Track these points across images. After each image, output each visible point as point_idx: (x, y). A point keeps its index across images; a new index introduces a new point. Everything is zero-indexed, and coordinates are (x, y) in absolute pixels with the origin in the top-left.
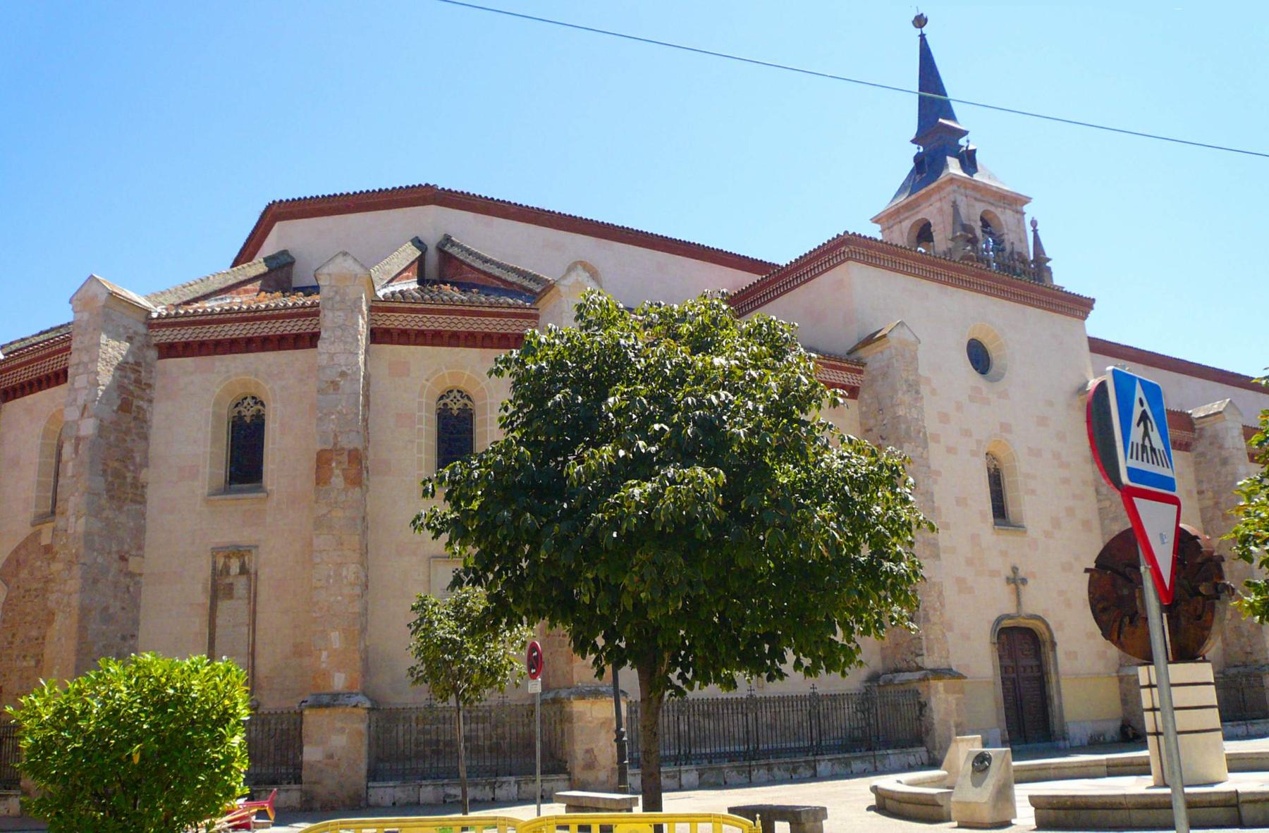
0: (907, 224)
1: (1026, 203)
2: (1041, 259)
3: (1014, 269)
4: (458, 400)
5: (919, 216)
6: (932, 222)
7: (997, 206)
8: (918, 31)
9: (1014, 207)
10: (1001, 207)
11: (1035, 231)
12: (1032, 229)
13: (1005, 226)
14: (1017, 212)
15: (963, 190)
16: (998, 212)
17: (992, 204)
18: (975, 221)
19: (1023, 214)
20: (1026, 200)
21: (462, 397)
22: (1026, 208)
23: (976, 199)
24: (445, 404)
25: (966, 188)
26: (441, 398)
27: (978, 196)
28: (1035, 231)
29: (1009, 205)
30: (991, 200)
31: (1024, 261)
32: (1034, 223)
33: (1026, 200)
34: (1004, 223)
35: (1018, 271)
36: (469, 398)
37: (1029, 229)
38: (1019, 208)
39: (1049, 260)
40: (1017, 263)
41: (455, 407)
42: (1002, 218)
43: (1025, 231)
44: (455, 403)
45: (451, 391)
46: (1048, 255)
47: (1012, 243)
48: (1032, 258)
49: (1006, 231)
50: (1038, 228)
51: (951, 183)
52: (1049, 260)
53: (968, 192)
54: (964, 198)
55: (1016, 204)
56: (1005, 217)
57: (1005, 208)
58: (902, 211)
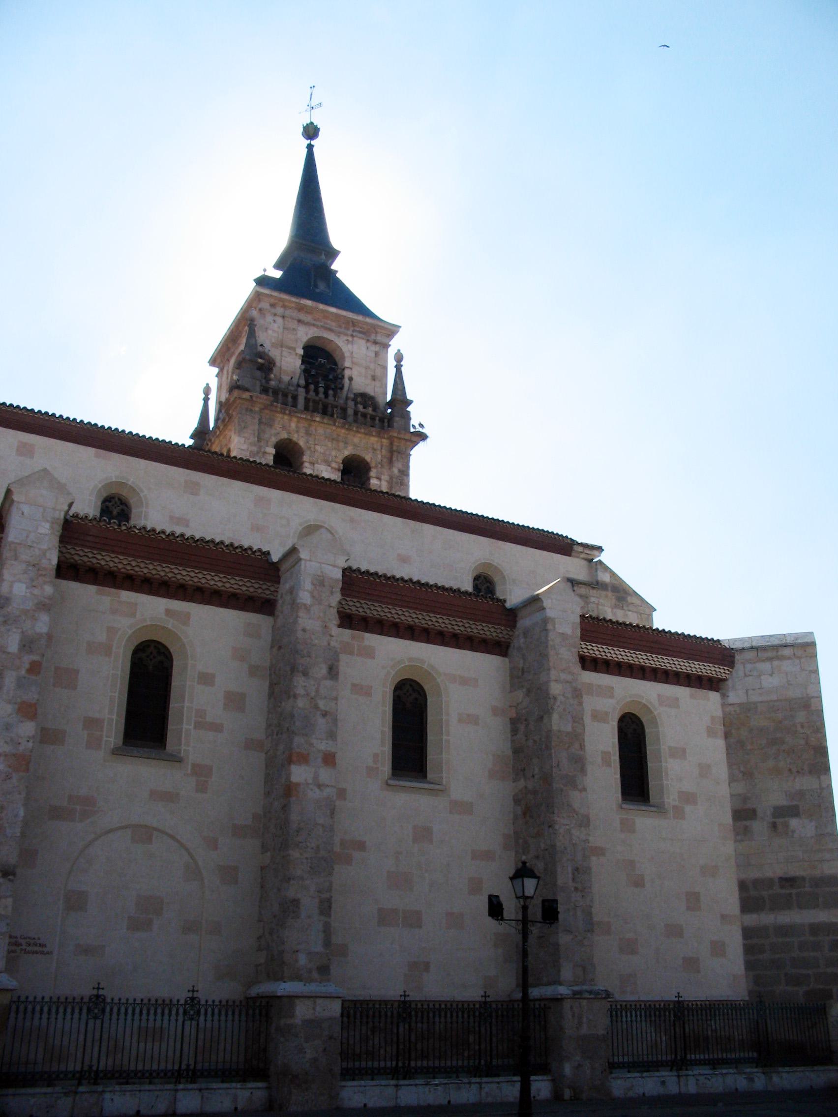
2: (400, 401)
7: (338, 334)
9: (373, 337)
10: (347, 335)
11: (398, 368)
12: (395, 363)
14: (375, 343)
18: (294, 349)
19: (386, 346)
23: (299, 321)
25: (284, 306)
28: (398, 368)
29: (360, 332)
30: (333, 325)
32: (399, 358)
33: (391, 331)
34: (347, 354)
38: (379, 338)
39: (409, 403)
42: (346, 348)
43: (385, 368)
46: (409, 396)
49: (347, 364)
53: (288, 312)
54: (280, 320)
55: (376, 333)
57: (352, 336)
58: (230, 345)
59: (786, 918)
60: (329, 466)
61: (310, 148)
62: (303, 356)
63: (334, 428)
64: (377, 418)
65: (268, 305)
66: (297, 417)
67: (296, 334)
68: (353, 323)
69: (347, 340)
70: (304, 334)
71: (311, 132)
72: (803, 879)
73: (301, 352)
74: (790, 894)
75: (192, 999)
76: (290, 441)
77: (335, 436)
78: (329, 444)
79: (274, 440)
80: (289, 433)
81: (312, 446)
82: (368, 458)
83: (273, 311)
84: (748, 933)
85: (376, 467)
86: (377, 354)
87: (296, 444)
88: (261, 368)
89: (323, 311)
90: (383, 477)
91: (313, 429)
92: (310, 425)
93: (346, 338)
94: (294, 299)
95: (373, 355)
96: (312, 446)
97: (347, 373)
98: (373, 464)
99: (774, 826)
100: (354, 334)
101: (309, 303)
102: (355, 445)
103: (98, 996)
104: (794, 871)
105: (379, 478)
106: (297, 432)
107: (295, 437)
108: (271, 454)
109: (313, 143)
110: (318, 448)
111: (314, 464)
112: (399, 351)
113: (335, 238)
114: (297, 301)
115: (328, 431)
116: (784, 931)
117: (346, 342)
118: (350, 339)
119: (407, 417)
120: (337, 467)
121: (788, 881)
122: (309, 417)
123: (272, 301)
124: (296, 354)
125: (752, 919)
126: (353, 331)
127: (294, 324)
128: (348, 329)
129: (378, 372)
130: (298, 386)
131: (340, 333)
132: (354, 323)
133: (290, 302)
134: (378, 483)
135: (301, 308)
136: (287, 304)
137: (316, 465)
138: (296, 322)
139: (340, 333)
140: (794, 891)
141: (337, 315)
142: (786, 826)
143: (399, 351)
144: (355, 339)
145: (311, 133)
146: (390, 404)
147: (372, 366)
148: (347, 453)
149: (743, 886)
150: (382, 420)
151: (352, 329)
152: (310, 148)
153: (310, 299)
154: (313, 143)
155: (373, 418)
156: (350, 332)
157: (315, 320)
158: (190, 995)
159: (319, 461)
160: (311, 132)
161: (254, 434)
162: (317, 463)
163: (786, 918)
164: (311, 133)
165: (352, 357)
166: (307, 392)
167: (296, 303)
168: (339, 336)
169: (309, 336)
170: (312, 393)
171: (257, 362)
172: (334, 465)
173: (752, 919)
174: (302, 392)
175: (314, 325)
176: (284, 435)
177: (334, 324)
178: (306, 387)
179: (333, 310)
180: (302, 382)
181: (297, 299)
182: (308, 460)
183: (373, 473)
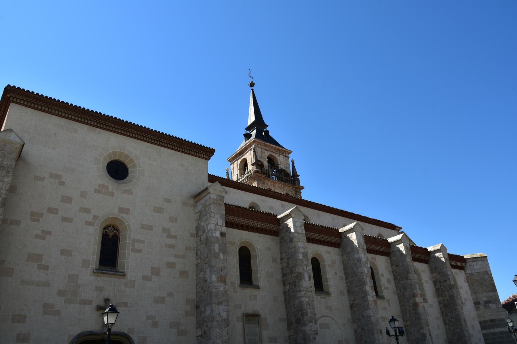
0: (239, 161)
1: (290, 153)
3: (282, 178)
4: (112, 231)
5: (243, 157)
6: (247, 159)
8: (251, 88)
10: (278, 154)
11: (293, 164)
13: (279, 162)
14: (285, 156)
15: (260, 146)
16: (276, 156)
18: (265, 159)
20: (290, 152)
21: (114, 230)
22: (289, 156)
23: (265, 150)
24: (106, 232)
25: (261, 145)
26: (105, 228)
27: (267, 149)
28: (293, 164)
29: (281, 153)
30: (274, 151)
31: (287, 174)
33: (290, 152)
34: (279, 160)
35: (284, 179)
36: (117, 231)
37: (291, 163)
38: (286, 155)
39: (299, 176)
40: (283, 176)
41: (111, 234)
42: (278, 158)
43: (289, 164)
44: (111, 232)
45: (109, 226)
49: (279, 163)
50: (294, 163)
51: (254, 143)
52: (299, 176)
53: (262, 147)
54: (260, 149)
55: (285, 153)
56: (280, 159)
57: (279, 154)
58: (238, 155)
59: (493, 331)
63: (281, 184)
64: (290, 181)
67: (265, 154)
68: (279, 150)
70: (267, 154)
71: (252, 85)
72: (496, 320)
74: (493, 324)
77: (281, 187)
78: (280, 190)
80: (269, 186)
84: (484, 335)
86: (286, 160)
88: (259, 165)
91: (275, 185)
92: (274, 184)
93: (278, 155)
94: (264, 143)
95: (285, 160)
99: (485, 306)
100: (280, 153)
101: (268, 144)
102: (286, 190)
104: (493, 318)
106: (271, 186)
107: (271, 188)
109: (253, 88)
112: (292, 159)
113: (266, 122)
114: (265, 143)
115: (279, 185)
116: (494, 334)
118: (279, 155)
121: (492, 321)
122: (280, 183)
123: (258, 143)
125: (485, 332)
126: (279, 153)
127: (264, 150)
128: (278, 152)
129: (287, 166)
131: (276, 153)
132: (279, 150)
133: (263, 143)
135: (265, 145)
136: (262, 144)
139: (276, 153)
140: (494, 323)
141: (275, 148)
142: (489, 306)
143: (292, 159)
145: (252, 85)
147: (285, 164)
149: (480, 323)
152: (252, 89)
153: (268, 142)
154: (253, 88)
155: (289, 181)
163: (493, 331)
164: (252, 85)
165: (280, 161)
168: (276, 154)
169: (269, 154)
171: (258, 163)
173: (485, 332)
175: (269, 151)
177: (274, 150)
179: (274, 146)
181: (265, 142)
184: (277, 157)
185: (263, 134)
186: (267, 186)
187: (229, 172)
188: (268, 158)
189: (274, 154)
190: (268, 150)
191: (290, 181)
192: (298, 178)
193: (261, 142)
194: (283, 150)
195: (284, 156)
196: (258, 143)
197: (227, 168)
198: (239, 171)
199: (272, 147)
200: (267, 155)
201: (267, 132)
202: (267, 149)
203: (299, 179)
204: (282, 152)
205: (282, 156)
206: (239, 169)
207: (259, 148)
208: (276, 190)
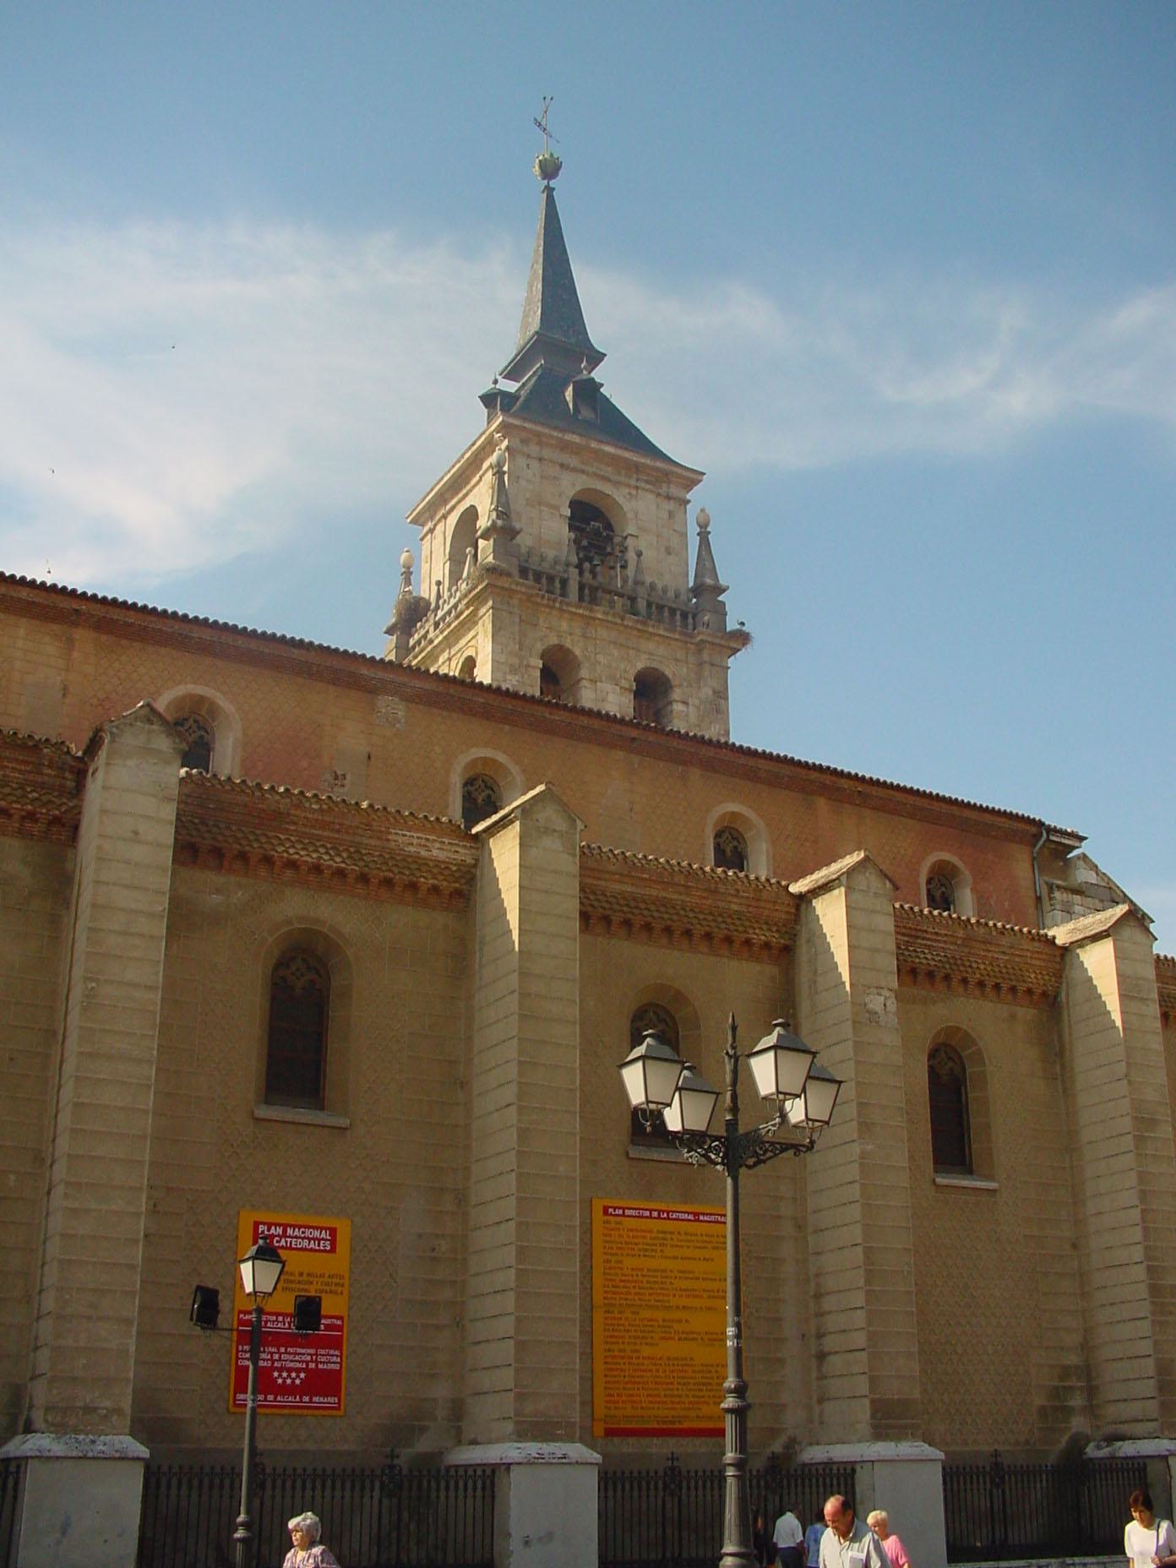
0: (453, 519)
2: (709, 590)
7: (617, 484)
10: (629, 486)
11: (704, 536)
14: (669, 498)
16: (619, 495)
17: (608, 480)
18: (557, 508)
25: (540, 443)
28: (704, 536)
29: (647, 482)
30: (608, 471)
33: (692, 478)
34: (630, 515)
37: (693, 530)
38: (674, 491)
42: (627, 506)
43: (684, 535)
47: (639, 554)
48: (691, 584)
49: (631, 529)
52: (723, 590)
54: (535, 464)
55: (669, 482)
60: (617, 685)
61: (549, 190)
62: (570, 519)
64: (678, 613)
65: (518, 441)
66: (571, 612)
69: (630, 494)
70: (571, 486)
71: (550, 170)
73: (568, 512)
75: (672, 1469)
76: (560, 647)
78: (616, 653)
79: (540, 647)
81: (593, 655)
82: (668, 672)
83: (525, 449)
85: (681, 686)
86: (671, 515)
87: (569, 651)
89: (596, 451)
90: (690, 701)
93: (627, 490)
95: (666, 515)
96: (593, 655)
97: (630, 542)
98: (675, 682)
101: (575, 438)
103: (672, 1469)
105: (685, 703)
107: (568, 644)
108: (538, 667)
109: (552, 184)
110: (600, 658)
111: (596, 682)
112: (702, 510)
117: (628, 497)
118: (634, 492)
119: (720, 611)
120: (627, 686)
123: (524, 435)
124: (561, 515)
126: (637, 480)
128: (630, 477)
130: (568, 565)
132: (637, 468)
133: (551, 436)
134: (685, 709)
135: (565, 447)
136: (544, 439)
137: (599, 684)
138: (558, 468)
141: (613, 457)
144: (639, 491)
146: (698, 590)
148: (640, 666)
150: (684, 616)
151: (635, 476)
152: (549, 190)
154: (552, 184)
156: (633, 482)
157: (583, 463)
158: (388, 1461)
159: (604, 678)
160: (550, 170)
161: (514, 639)
162: (601, 681)
166: (581, 573)
167: (557, 438)
169: (578, 488)
170: (587, 575)
172: (624, 683)
174: (573, 573)
175: (583, 472)
176: (554, 641)
178: (579, 566)
180: (574, 559)
182: (587, 677)
183: (676, 694)
184: (620, 500)
185: (569, 394)
186: (546, 636)
187: (411, 573)
188: (574, 504)
189: (607, 489)
190: (574, 470)
191: (678, 613)
192: (720, 598)
193: (539, 428)
194: (657, 469)
195: (659, 495)
196: (524, 435)
197: (404, 556)
198: (448, 564)
199: (599, 456)
200: (571, 493)
201: (590, 392)
202: (574, 461)
203: (723, 604)
204: (648, 475)
205: (651, 497)
206: (447, 557)
207: (529, 456)
208: (596, 654)
